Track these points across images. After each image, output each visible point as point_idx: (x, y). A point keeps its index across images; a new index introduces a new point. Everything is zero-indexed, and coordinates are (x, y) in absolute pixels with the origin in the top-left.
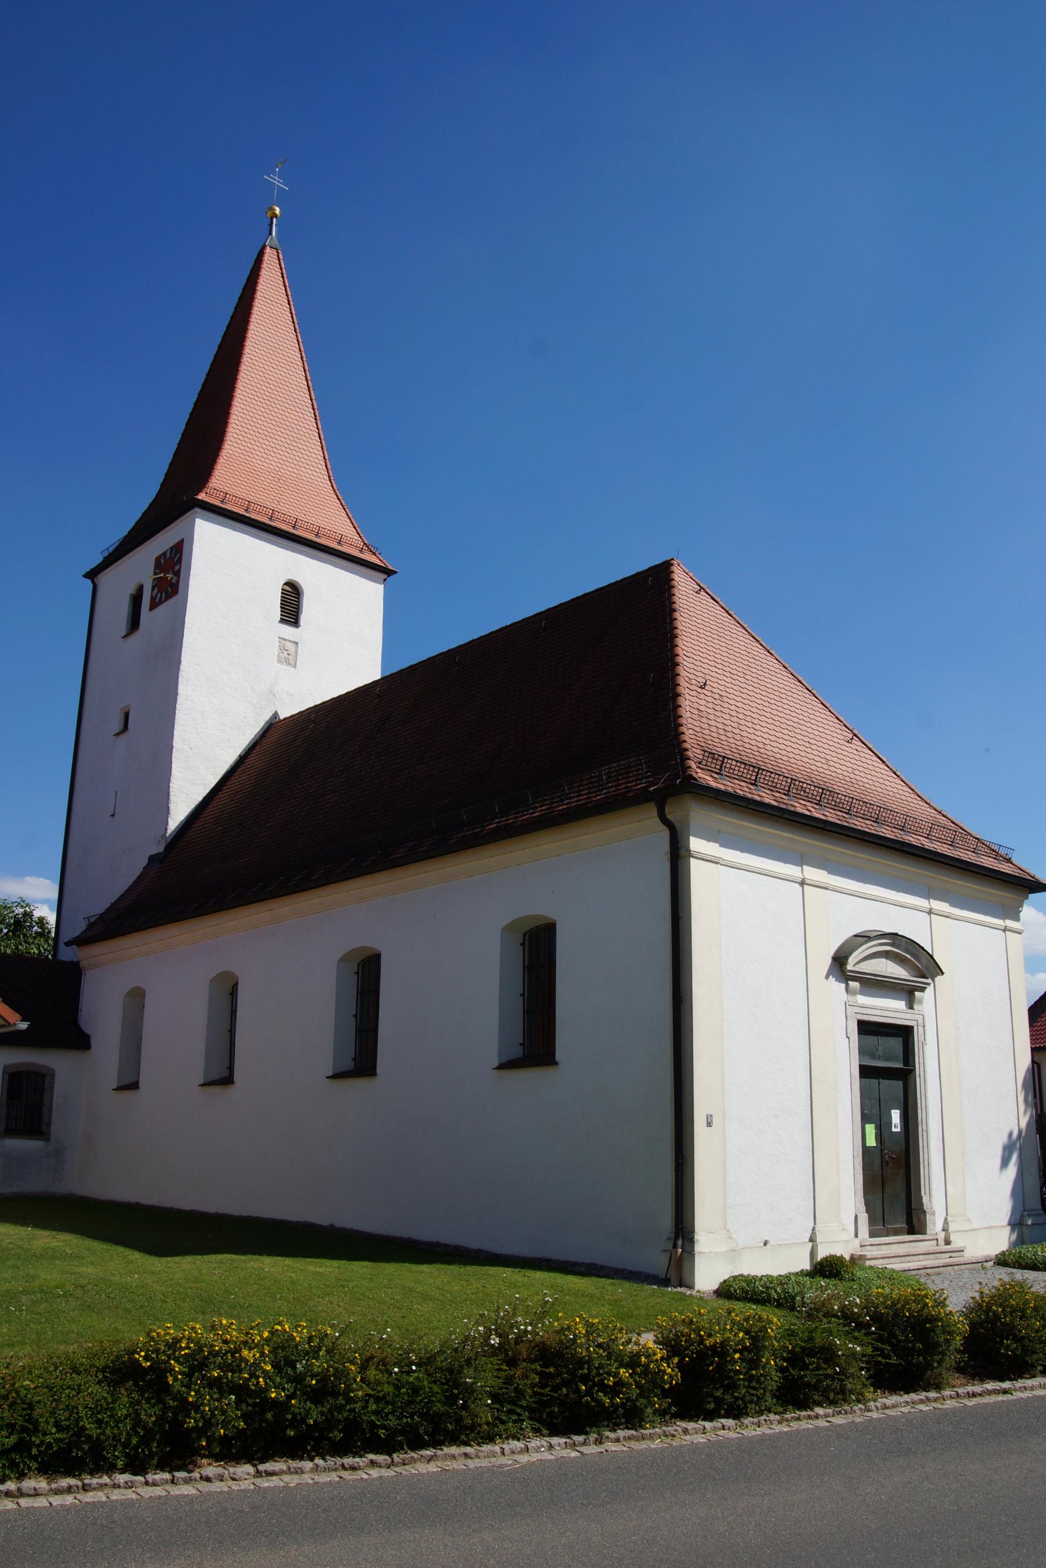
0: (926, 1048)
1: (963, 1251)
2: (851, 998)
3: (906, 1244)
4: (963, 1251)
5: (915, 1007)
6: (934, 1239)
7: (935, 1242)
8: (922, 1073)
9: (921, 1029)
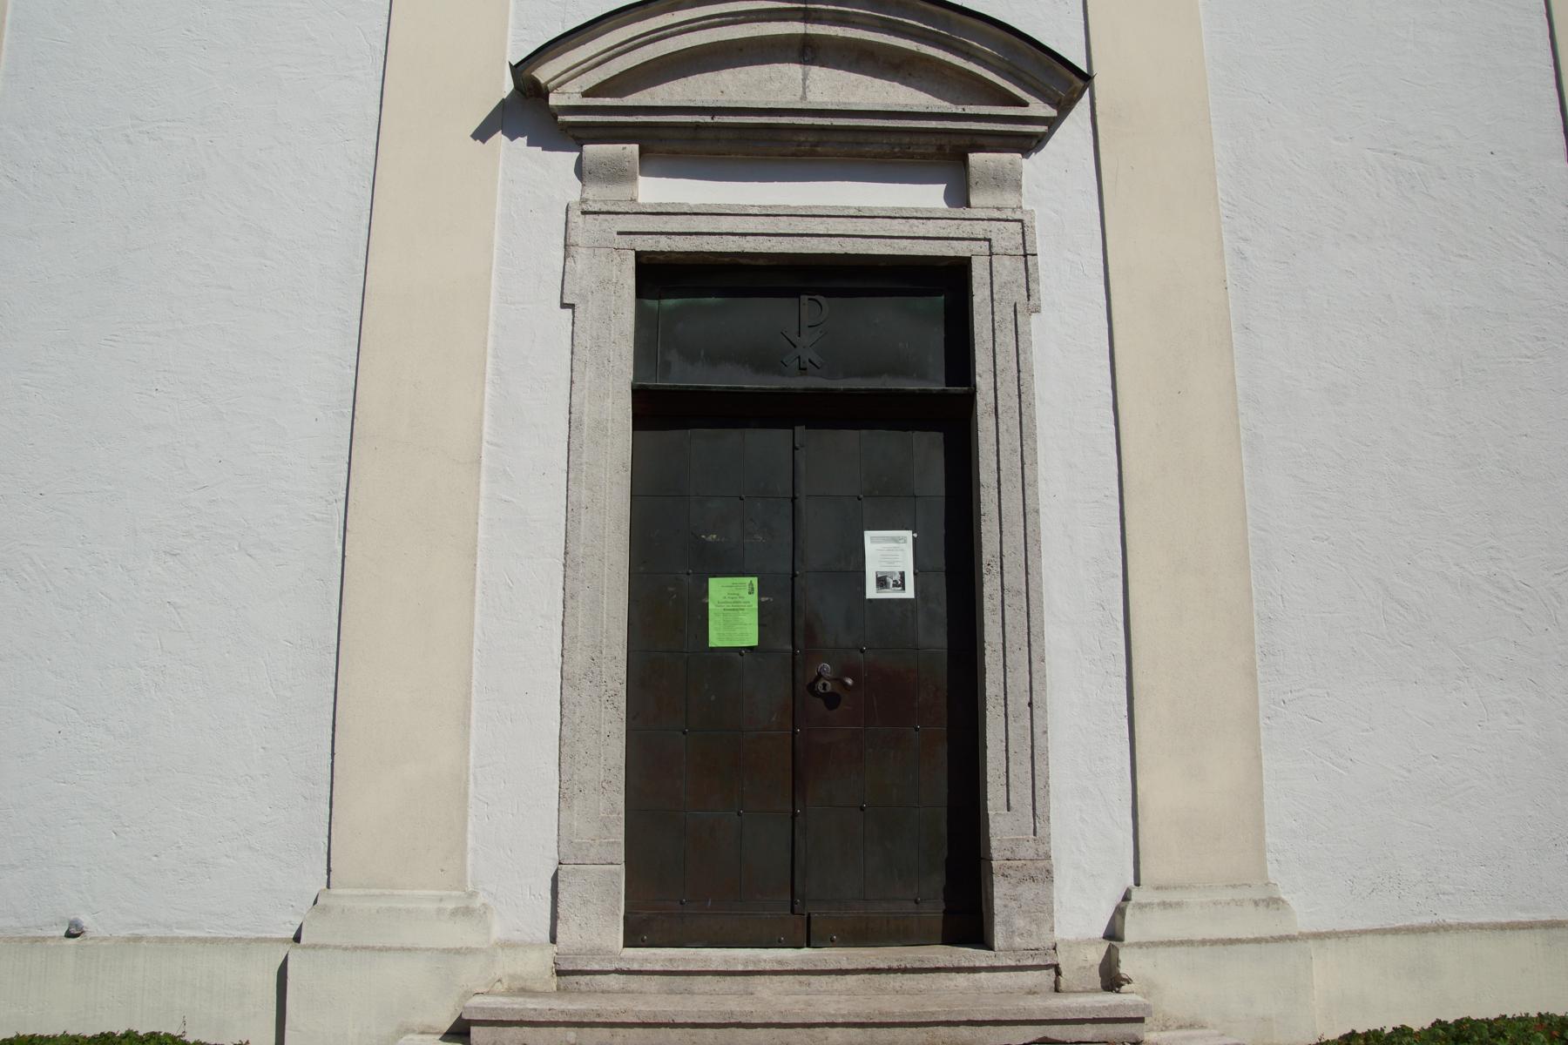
0: (1035, 326)
1: (1141, 1020)
2: (600, 194)
3: (851, 980)
4: (1141, 1020)
5: (973, 201)
6: (1047, 967)
7: (1047, 977)
8: (1008, 402)
9: (1007, 269)
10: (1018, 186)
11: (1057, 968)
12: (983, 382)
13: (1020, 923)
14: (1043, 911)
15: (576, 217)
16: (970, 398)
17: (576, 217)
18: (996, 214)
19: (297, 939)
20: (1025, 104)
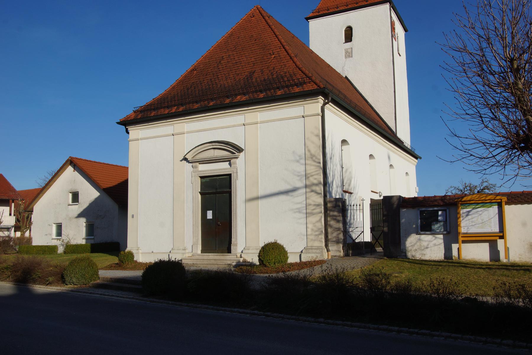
0: (237, 182)
9: (235, 174)
10: (236, 164)
11: (237, 255)
12: (232, 189)
13: (234, 251)
14: (236, 249)
15: (193, 173)
16: (231, 191)
17: (193, 173)
18: (234, 168)
19: (170, 252)
20: (235, 154)
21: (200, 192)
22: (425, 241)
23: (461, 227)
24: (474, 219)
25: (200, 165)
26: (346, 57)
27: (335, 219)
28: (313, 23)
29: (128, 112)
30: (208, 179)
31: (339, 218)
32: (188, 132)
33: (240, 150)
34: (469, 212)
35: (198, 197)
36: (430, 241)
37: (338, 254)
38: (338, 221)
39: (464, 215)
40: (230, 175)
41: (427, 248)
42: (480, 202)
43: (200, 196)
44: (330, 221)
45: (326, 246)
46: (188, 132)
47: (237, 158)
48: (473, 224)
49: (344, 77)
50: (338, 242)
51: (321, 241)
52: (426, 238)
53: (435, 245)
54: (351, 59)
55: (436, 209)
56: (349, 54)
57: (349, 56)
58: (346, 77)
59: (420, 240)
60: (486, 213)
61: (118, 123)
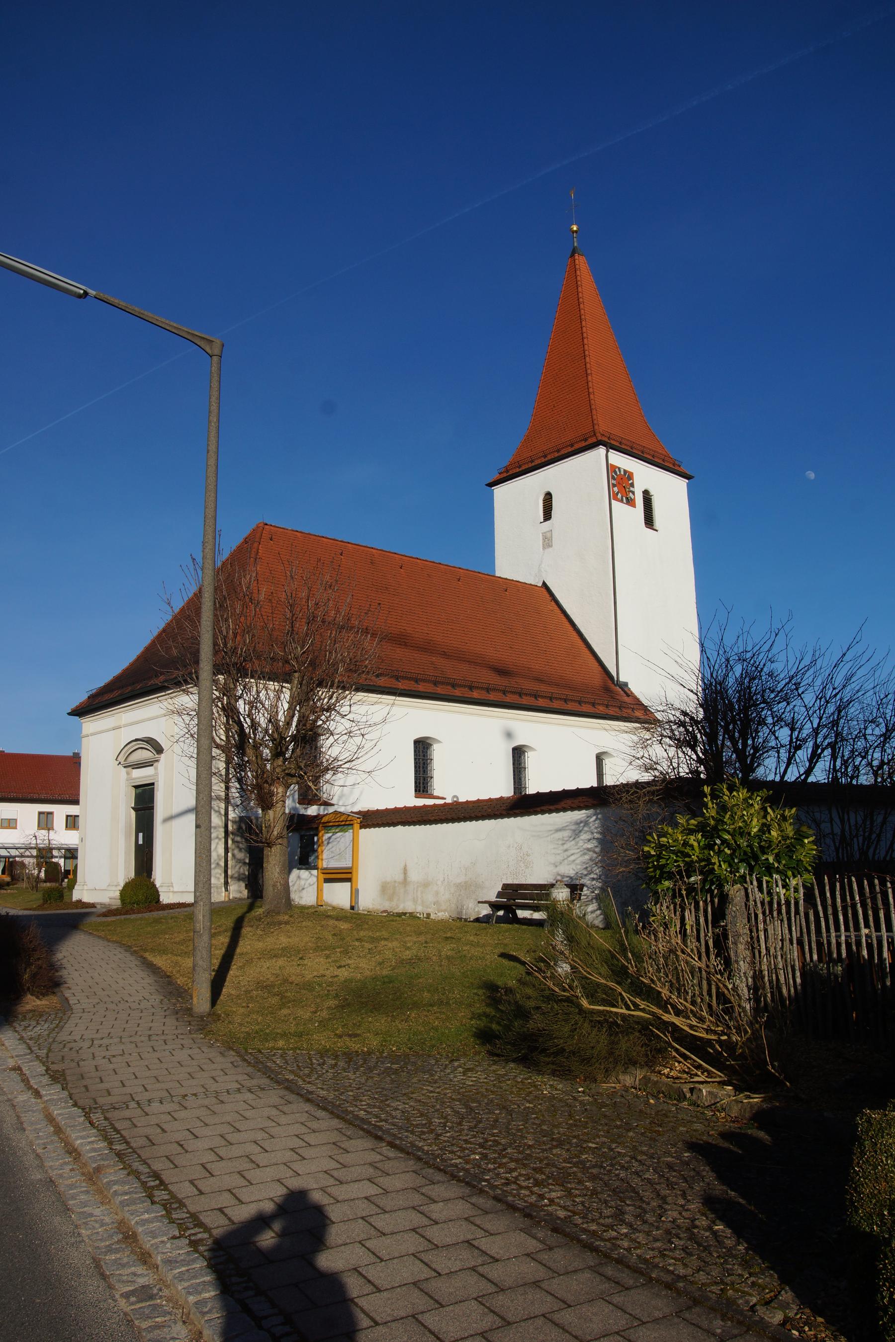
21: (133, 808)
22: (303, 879)
23: (322, 860)
24: (333, 849)
25: (134, 770)
26: (544, 548)
27: (238, 847)
28: (500, 492)
29: (80, 697)
30: (140, 790)
31: (241, 845)
32: (125, 726)
33: (159, 750)
34: (330, 838)
35: (130, 815)
36: (307, 880)
37: (238, 895)
38: (240, 850)
39: (325, 843)
40: (153, 784)
41: (303, 889)
42: (337, 824)
43: (133, 813)
44: (233, 850)
45: (226, 883)
46: (125, 726)
47: (157, 761)
48: (333, 855)
49: (540, 584)
50: (239, 879)
51: (219, 878)
52: (304, 874)
53: (310, 885)
54: (550, 549)
55: (312, 833)
56: (547, 542)
57: (550, 546)
58: (544, 584)
59: (299, 877)
60: (343, 839)
61: (69, 714)
